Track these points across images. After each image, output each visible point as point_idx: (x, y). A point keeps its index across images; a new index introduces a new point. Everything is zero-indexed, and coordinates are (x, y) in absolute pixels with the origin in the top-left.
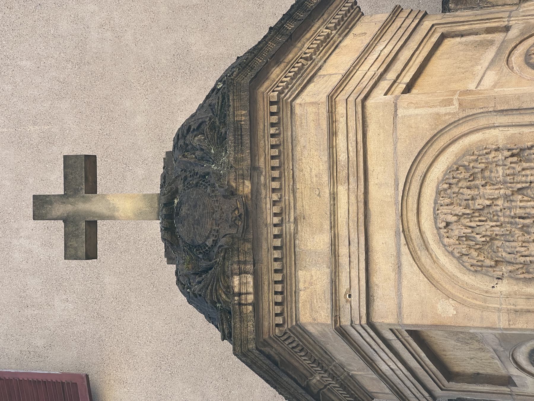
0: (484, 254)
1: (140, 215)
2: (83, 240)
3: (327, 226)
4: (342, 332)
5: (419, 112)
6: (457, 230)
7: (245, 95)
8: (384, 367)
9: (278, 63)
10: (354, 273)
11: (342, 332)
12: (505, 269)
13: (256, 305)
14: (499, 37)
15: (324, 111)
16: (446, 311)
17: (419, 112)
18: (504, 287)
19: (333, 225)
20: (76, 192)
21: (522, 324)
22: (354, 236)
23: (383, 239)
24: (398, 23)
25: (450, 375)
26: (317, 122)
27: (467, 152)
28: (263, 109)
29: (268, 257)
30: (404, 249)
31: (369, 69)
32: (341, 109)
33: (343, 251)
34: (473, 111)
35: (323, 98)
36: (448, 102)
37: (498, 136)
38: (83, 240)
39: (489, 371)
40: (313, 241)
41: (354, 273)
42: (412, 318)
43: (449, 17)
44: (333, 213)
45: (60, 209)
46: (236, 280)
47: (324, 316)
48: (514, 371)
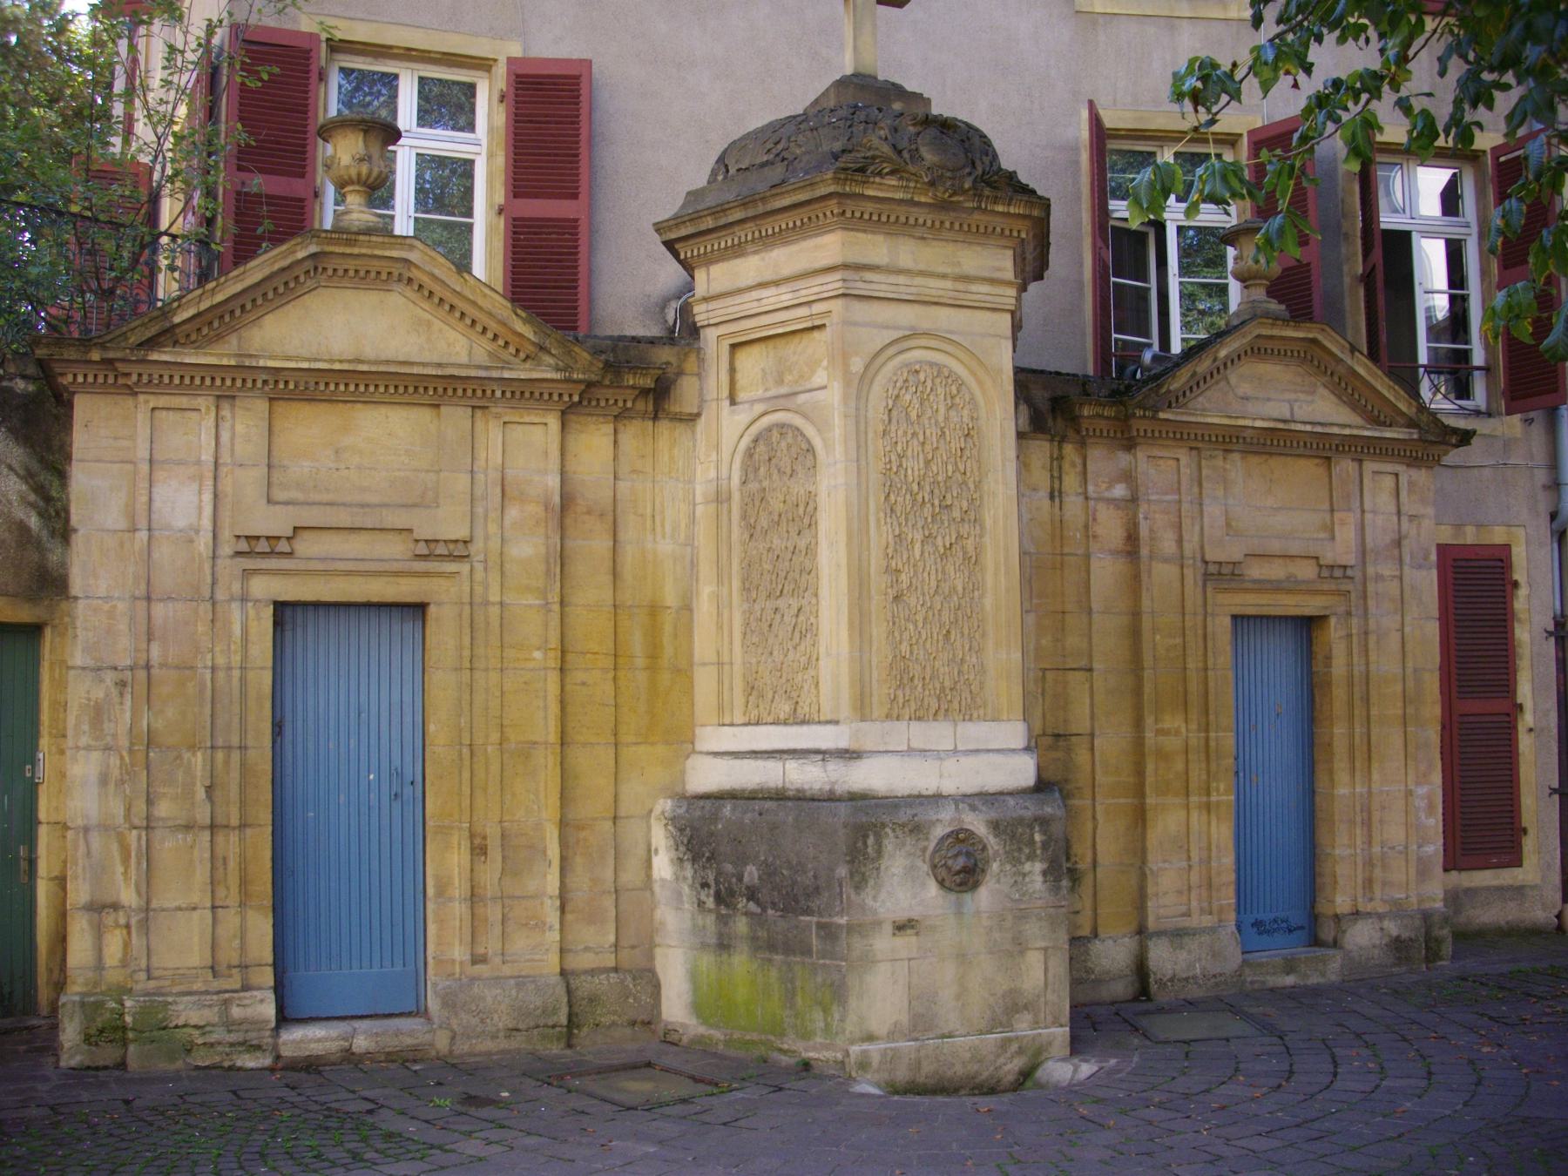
10: (883, 287)
19: (922, 273)
22: (913, 290)
23: (907, 316)
33: (901, 279)
41: (883, 287)
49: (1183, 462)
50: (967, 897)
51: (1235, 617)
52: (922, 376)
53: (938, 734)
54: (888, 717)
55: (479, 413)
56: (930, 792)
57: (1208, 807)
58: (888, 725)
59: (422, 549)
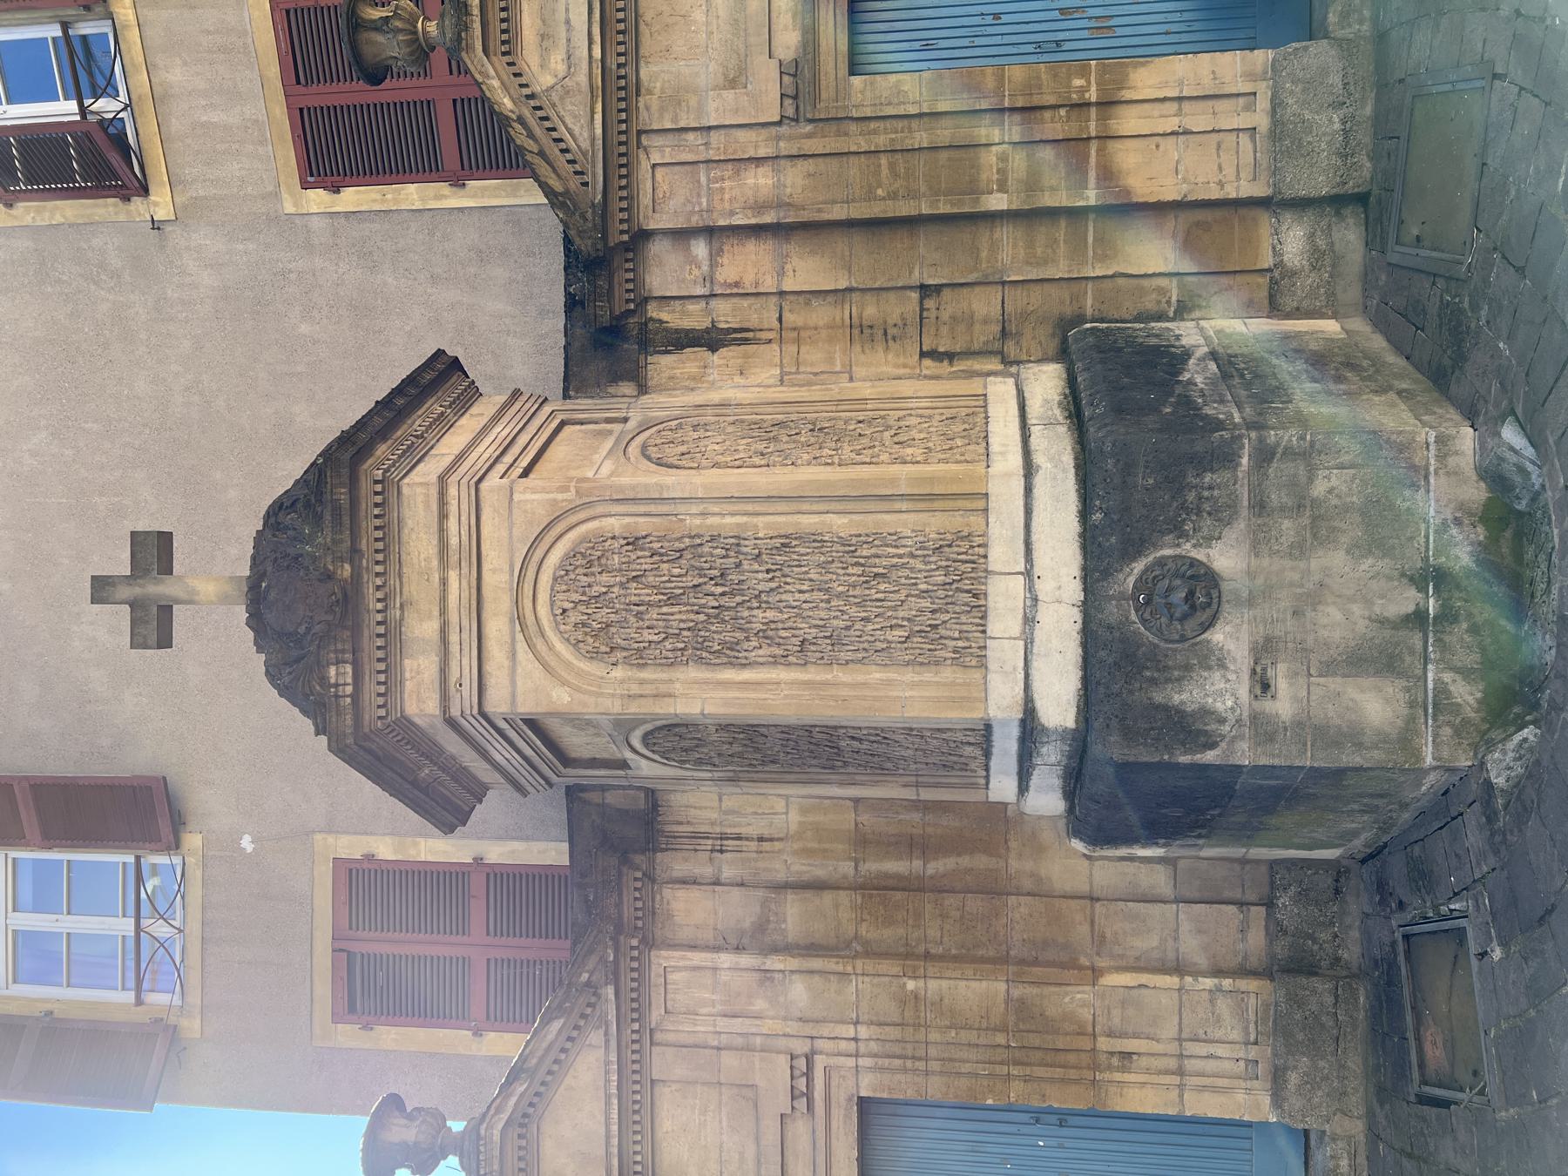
0: (599, 640)
1: (224, 599)
2: (154, 626)
3: (436, 613)
4: (451, 723)
5: (535, 497)
6: (574, 617)
7: (345, 471)
8: (498, 757)
9: (384, 439)
10: (465, 661)
11: (451, 723)
12: (620, 655)
13: (355, 697)
14: (617, 427)
15: (434, 492)
16: (561, 698)
17: (535, 497)
18: (618, 673)
19: (443, 612)
20: (147, 572)
21: (634, 708)
22: (465, 623)
23: (497, 627)
24: (517, 405)
25: (566, 761)
26: (427, 505)
27: (584, 539)
28: (365, 486)
29: (370, 645)
30: (519, 636)
31: (486, 450)
32: (452, 491)
33: (454, 638)
34: (589, 500)
35: (434, 478)
36: (565, 489)
37: (614, 524)
38: (154, 626)
39: (605, 755)
40: (421, 628)
41: (465, 661)
42: (526, 707)
43: (569, 404)
44: (443, 598)
45: (125, 592)
46: (332, 671)
47: (432, 706)
48: (628, 755)
49: (656, 158)
50: (1225, 586)
51: (853, 72)
52: (567, 605)
53: (1005, 596)
54: (982, 664)
55: (658, 1036)
56: (1078, 617)
57: (1108, 104)
58: (992, 666)
59: (802, 1104)
